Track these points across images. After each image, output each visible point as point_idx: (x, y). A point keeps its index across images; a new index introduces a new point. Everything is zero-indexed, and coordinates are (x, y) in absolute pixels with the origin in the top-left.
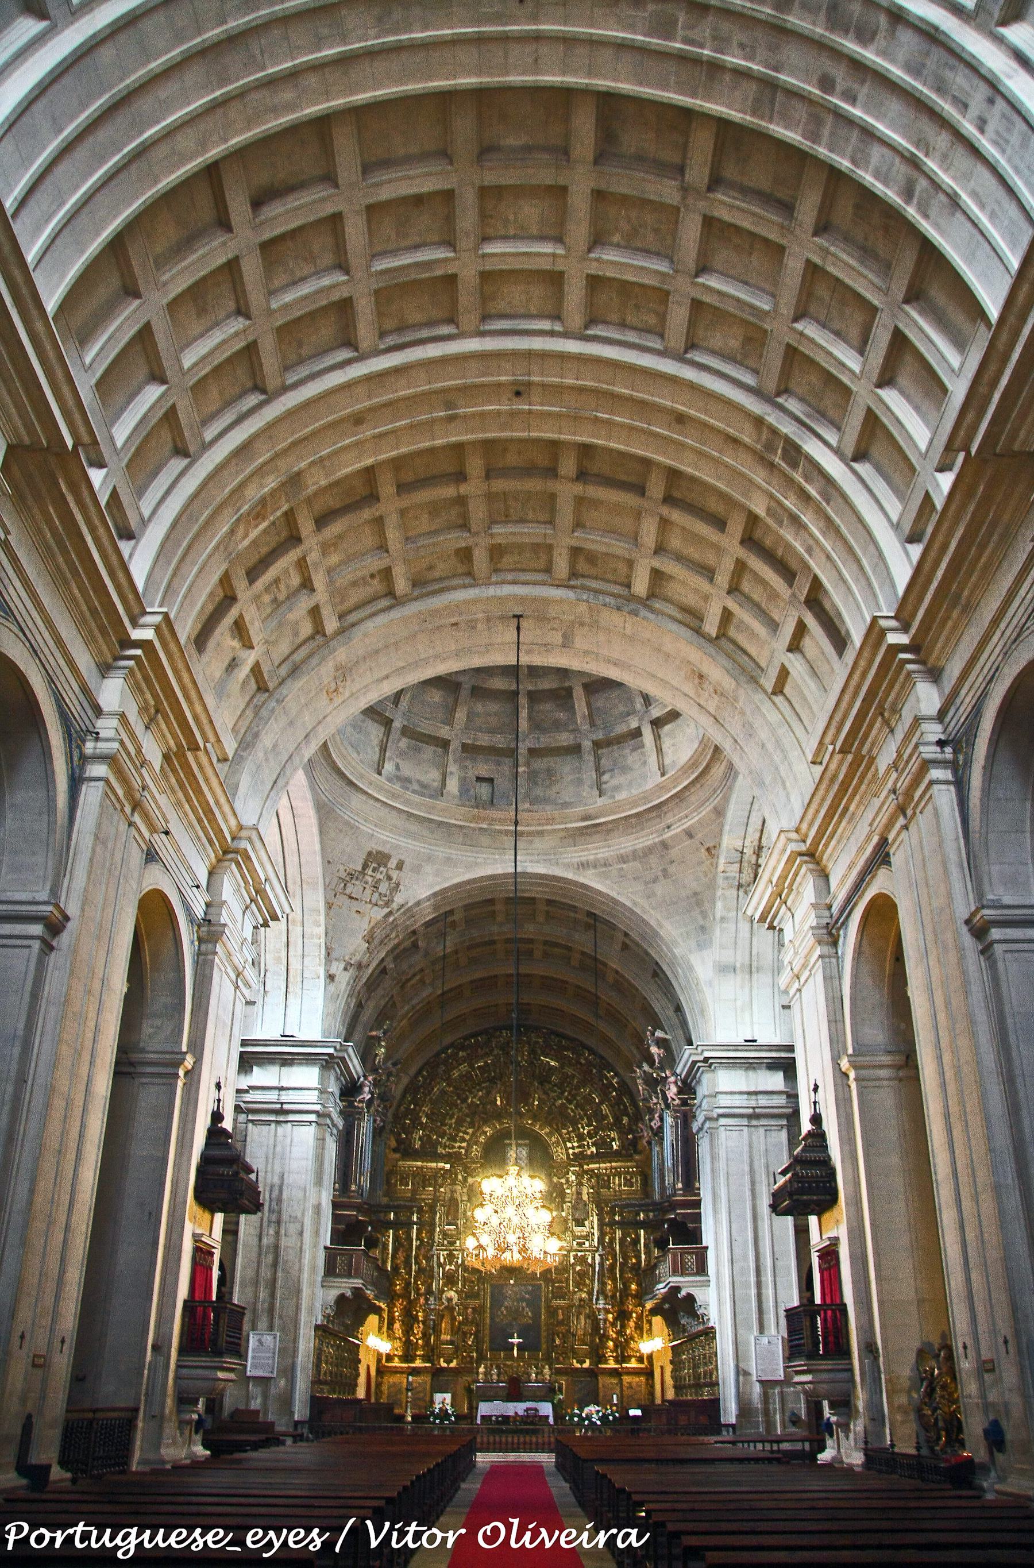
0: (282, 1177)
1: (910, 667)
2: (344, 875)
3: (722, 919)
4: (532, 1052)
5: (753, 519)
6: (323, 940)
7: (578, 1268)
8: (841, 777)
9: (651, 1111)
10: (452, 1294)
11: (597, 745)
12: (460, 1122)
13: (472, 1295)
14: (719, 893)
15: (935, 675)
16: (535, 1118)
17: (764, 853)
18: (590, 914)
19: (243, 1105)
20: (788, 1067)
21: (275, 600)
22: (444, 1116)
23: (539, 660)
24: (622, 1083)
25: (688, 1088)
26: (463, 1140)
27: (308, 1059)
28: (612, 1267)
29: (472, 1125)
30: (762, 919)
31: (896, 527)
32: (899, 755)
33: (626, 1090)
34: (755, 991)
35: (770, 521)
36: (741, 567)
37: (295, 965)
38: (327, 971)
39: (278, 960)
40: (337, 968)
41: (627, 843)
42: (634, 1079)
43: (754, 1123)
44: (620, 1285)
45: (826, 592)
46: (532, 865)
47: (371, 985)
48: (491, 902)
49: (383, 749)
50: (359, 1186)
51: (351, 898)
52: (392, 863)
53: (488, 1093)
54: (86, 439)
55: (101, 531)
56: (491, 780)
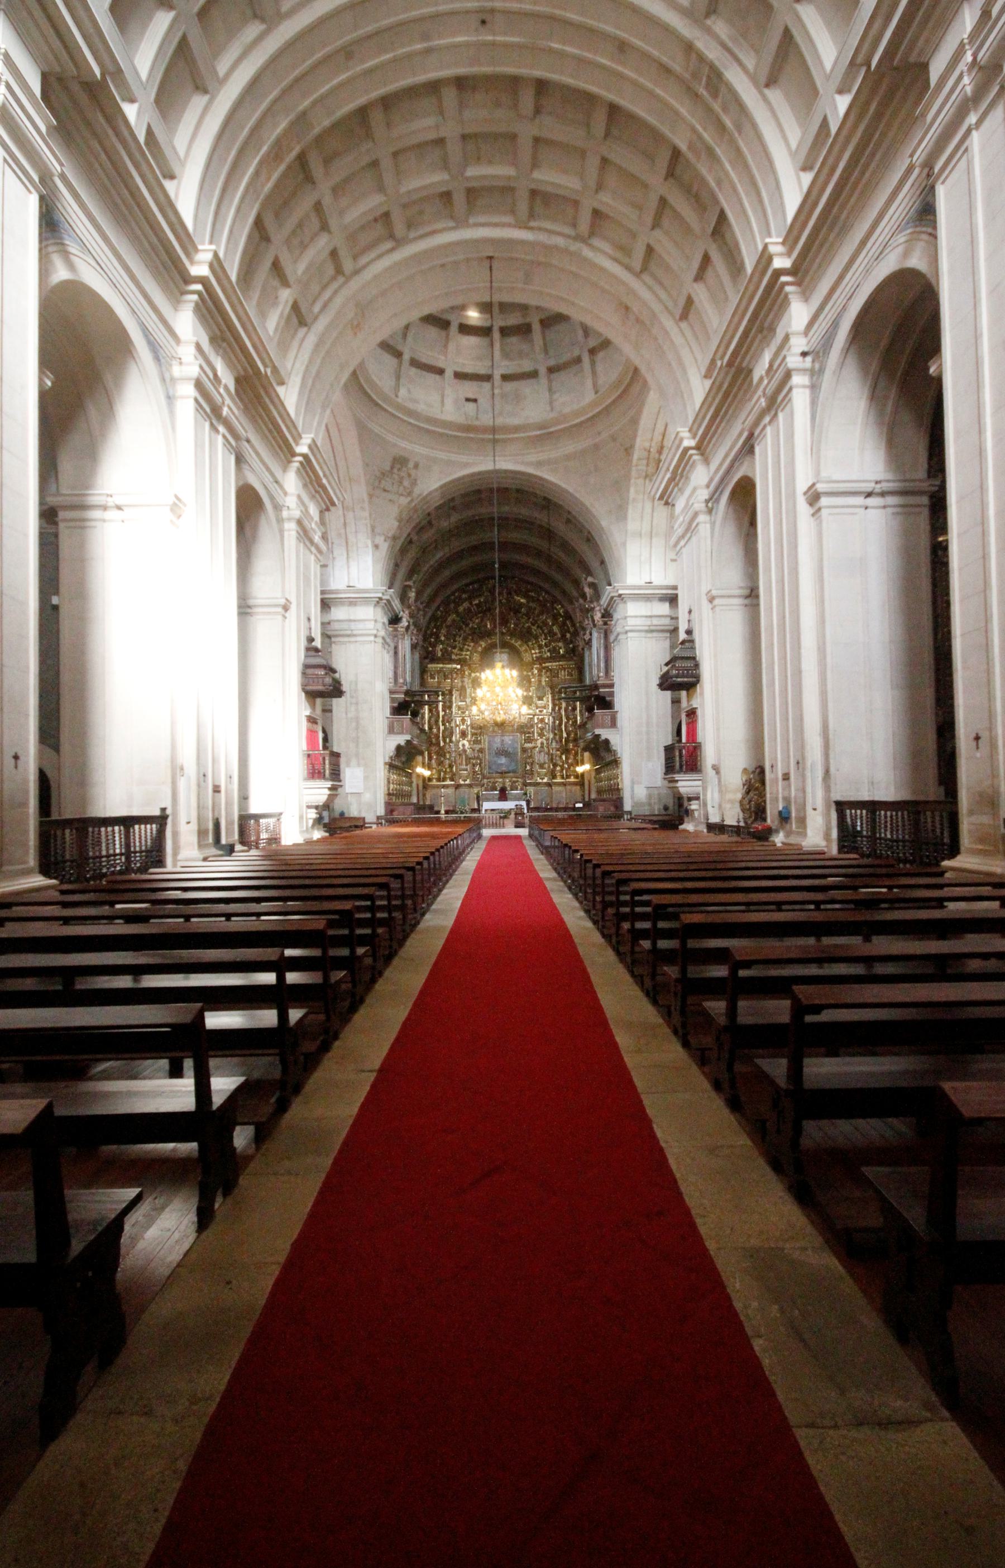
0: (356, 675)
1: (788, 289)
2: (378, 474)
3: (634, 500)
4: (509, 593)
5: (676, 154)
6: (368, 521)
8: (725, 386)
9: (584, 629)
10: (465, 742)
11: (551, 370)
12: (465, 639)
13: (477, 742)
14: (632, 481)
15: (806, 297)
16: (512, 634)
17: (665, 451)
18: (545, 498)
19: (329, 633)
20: (673, 600)
21: (302, 242)
22: (455, 636)
23: (506, 298)
24: (566, 612)
25: (607, 615)
26: (468, 650)
27: (366, 601)
28: (560, 724)
29: (473, 640)
30: (661, 498)
31: (793, 155)
32: (771, 365)
33: (568, 616)
34: (653, 549)
35: (690, 155)
36: (663, 201)
37: (352, 538)
38: (373, 542)
39: (339, 535)
40: (380, 540)
41: (569, 447)
42: (574, 609)
43: (649, 635)
44: (565, 735)
45: (729, 225)
46: (506, 464)
47: (403, 551)
48: (479, 491)
49: (398, 378)
50: (405, 680)
51: (385, 490)
52: (411, 465)
53: (482, 620)
54: (111, 68)
55: (149, 176)
56: (475, 401)
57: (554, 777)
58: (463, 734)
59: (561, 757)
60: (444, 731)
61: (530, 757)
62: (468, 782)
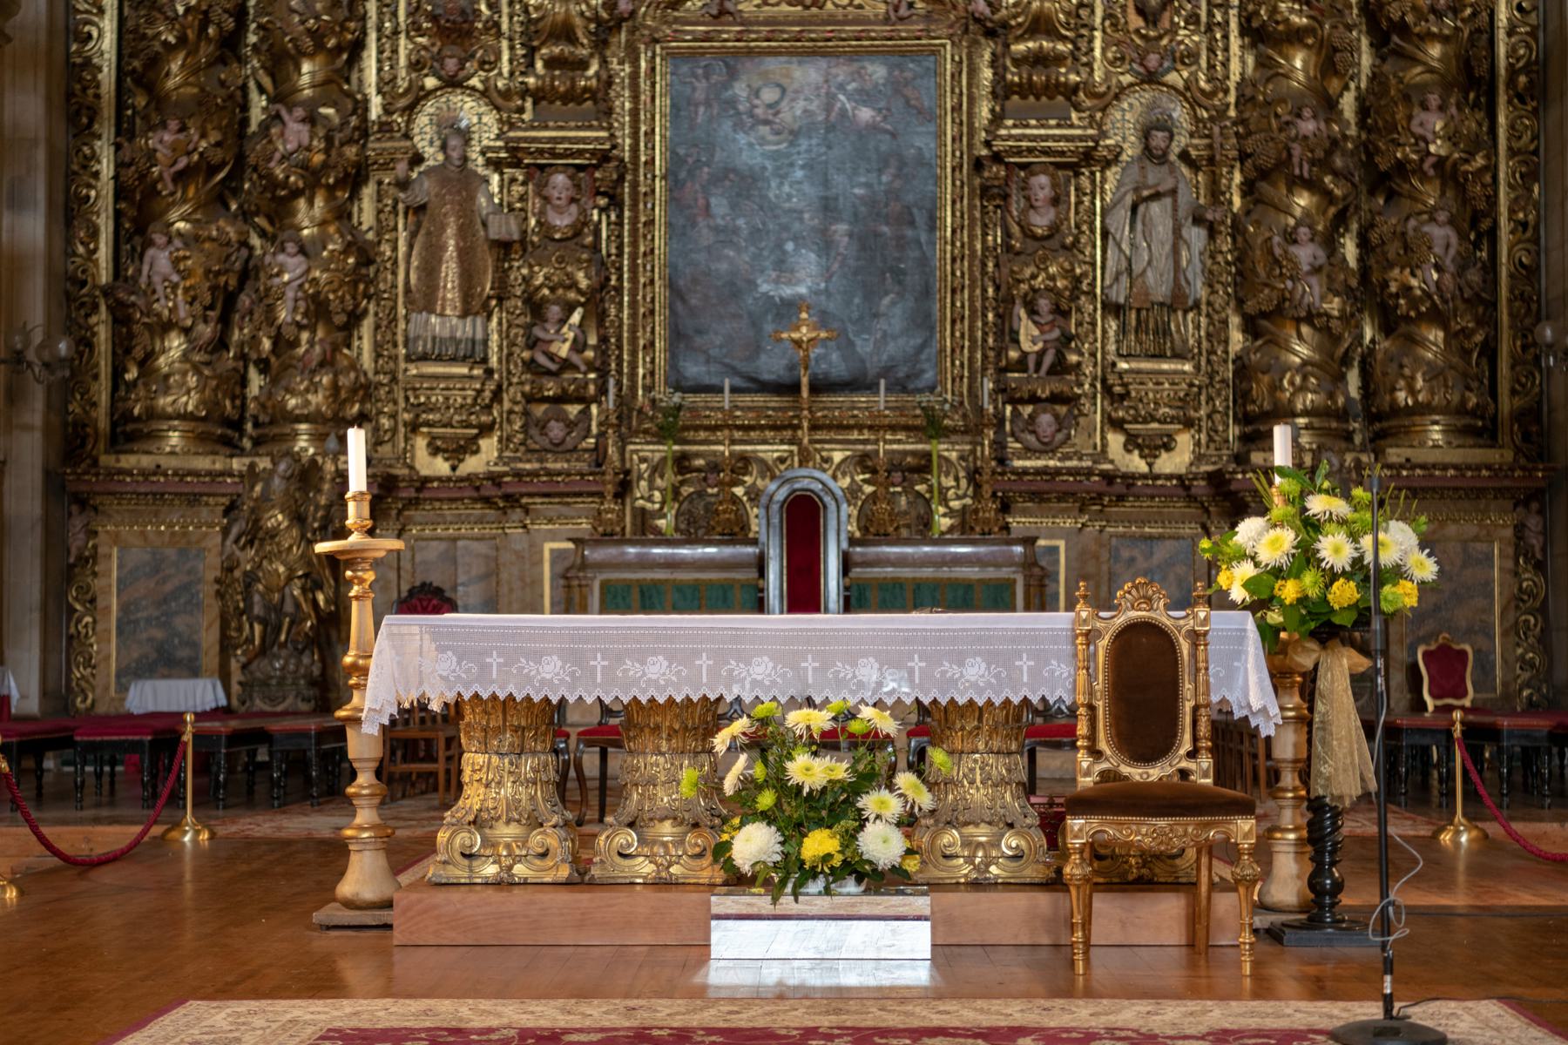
59: (1330, 243)
61: (1057, 242)
62: (486, 457)
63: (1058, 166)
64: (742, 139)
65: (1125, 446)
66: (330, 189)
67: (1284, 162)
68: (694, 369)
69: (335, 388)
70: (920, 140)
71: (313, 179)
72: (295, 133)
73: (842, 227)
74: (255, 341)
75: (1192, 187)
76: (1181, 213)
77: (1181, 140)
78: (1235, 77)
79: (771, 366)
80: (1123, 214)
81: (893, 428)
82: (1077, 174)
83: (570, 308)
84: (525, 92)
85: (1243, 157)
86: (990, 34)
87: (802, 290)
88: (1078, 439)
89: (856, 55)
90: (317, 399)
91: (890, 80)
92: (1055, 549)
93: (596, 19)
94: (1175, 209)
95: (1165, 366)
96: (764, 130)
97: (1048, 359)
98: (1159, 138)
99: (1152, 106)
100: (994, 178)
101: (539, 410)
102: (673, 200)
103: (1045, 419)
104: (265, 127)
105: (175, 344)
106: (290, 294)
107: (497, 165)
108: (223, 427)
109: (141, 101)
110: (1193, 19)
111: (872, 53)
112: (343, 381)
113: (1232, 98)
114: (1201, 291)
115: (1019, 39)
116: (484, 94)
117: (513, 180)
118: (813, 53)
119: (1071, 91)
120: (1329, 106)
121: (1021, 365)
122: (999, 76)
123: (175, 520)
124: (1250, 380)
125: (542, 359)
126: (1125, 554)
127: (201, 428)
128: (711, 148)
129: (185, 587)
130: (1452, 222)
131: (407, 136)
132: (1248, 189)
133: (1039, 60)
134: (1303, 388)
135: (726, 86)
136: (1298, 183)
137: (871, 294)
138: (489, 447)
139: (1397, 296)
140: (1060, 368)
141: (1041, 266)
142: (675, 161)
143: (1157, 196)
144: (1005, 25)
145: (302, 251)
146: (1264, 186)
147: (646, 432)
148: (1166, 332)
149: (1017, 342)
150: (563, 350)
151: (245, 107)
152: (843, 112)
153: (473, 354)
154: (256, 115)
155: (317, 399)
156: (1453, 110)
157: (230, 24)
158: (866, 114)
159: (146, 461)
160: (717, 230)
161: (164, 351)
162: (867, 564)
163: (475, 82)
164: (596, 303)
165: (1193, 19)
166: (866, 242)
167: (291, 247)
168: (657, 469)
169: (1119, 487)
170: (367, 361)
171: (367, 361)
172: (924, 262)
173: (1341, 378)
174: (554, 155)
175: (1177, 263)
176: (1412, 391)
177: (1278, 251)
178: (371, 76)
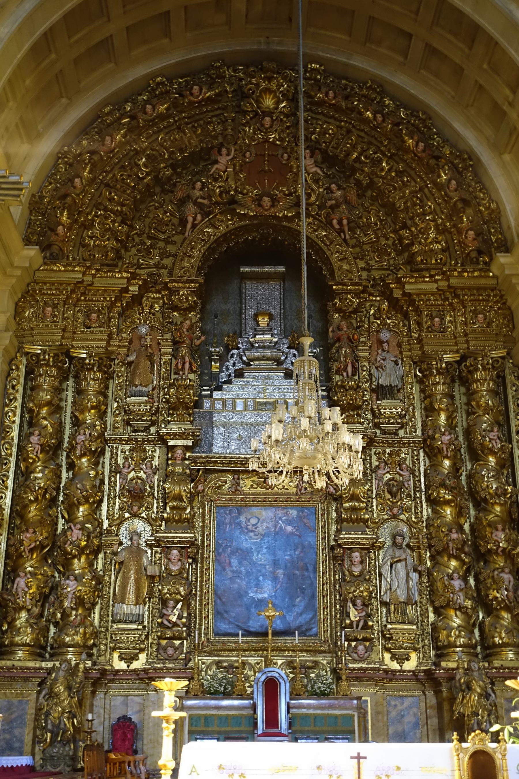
7: (388, 476)
10: (139, 525)
26: (164, 255)
57: (442, 651)
58: (136, 496)
59: (465, 579)
60: (70, 481)
63: (362, 549)
64: (243, 537)
65: (391, 658)
66: (88, 555)
67: (446, 549)
68: (224, 627)
69: (85, 633)
70: (310, 539)
71: (82, 551)
72: (76, 534)
73: (280, 572)
74: (54, 614)
75: (411, 557)
76: (409, 567)
77: (407, 540)
78: (425, 517)
79: (254, 625)
80: (387, 567)
81: (301, 651)
82: (369, 552)
83: (177, 602)
84: (163, 519)
85: (430, 547)
86: (335, 500)
87: (266, 595)
88: (373, 656)
89: (285, 507)
90: (78, 638)
91: (298, 516)
92: (366, 701)
93: (191, 493)
94: (406, 566)
95: (406, 627)
96: (251, 534)
97: (361, 624)
98: (399, 539)
99: (396, 527)
100: (338, 553)
101: (164, 642)
102: (217, 560)
103: (361, 648)
104: (64, 531)
105: (23, 615)
106: (70, 596)
107: (151, 546)
108: (39, 650)
109: (18, 522)
110: (409, 495)
111: (292, 506)
112: (87, 630)
113: (424, 525)
114: (417, 598)
115: (346, 502)
116: (148, 520)
117: (156, 552)
118: (270, 506)
119: (365, 521)
120: (460, 529)
121: (351, 626)
122: (339, 515)
123: (18, 688)
124: (439, 633)
125: (166, 622)
126: (393, 703)
127: (32, 649)
128: (231, 540)
129: (20, 716)
130: (510, 573)
131: (117, 535)
132: (432, 558)
133: (354, 509)
134: (459, 636)
135: (237, 517)
136: (451, 556)
137: (292, 598)
138: (143, 657)
139: (492, 600)
140: (366, 627)
141: (357, 587)
142: (218, 545)
143: (400, 561)
144: (341, 497)
145: (76, 579)
146: (439, 558)
147: (205, 652)
148: (406, 613)
149: (349, 617)
150: (174, 619)
151: (56, 524)
152: (281, 527)
153: (138, 620)
154: (60, 527)
155: (78, 638)
156: (507, 531)
157: (55, 493)
158: (289, 528)
159: (9, 663)
160: (233, 572)
161: (19, 618)
162: (295, 707)
163: (143, 515)
164: (187, 600)
165: (409, 495)
166: (290, 577)
167: (72, 578)
168: (209, 667)
169: (390, 676)
170: (96, 622)
171: (96, 622)
172: (312, 584)
173: (472, 632)
174: (173, 542)
175: (408, 587)
176: (501, 638)
177: (446, 583)
178: (104, 512)
